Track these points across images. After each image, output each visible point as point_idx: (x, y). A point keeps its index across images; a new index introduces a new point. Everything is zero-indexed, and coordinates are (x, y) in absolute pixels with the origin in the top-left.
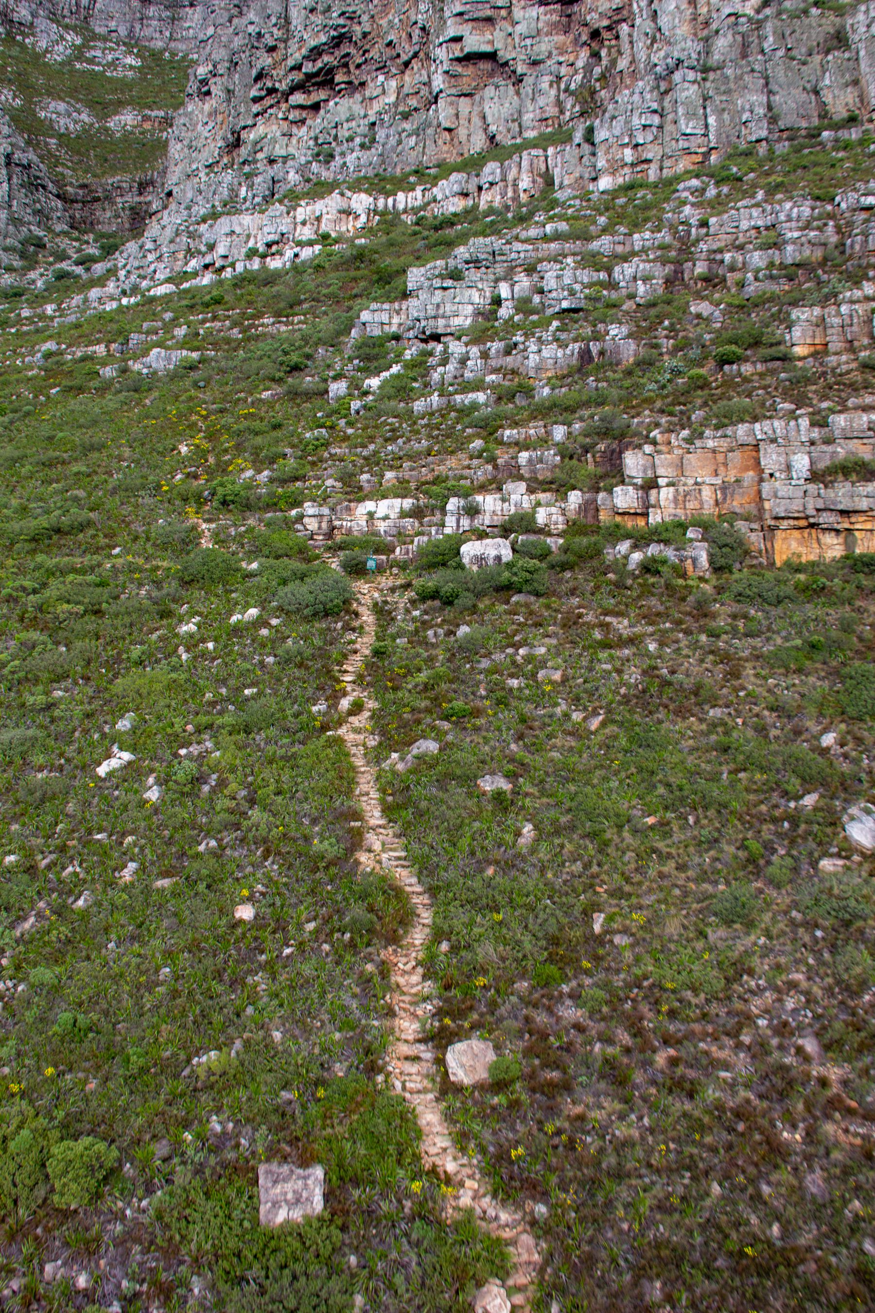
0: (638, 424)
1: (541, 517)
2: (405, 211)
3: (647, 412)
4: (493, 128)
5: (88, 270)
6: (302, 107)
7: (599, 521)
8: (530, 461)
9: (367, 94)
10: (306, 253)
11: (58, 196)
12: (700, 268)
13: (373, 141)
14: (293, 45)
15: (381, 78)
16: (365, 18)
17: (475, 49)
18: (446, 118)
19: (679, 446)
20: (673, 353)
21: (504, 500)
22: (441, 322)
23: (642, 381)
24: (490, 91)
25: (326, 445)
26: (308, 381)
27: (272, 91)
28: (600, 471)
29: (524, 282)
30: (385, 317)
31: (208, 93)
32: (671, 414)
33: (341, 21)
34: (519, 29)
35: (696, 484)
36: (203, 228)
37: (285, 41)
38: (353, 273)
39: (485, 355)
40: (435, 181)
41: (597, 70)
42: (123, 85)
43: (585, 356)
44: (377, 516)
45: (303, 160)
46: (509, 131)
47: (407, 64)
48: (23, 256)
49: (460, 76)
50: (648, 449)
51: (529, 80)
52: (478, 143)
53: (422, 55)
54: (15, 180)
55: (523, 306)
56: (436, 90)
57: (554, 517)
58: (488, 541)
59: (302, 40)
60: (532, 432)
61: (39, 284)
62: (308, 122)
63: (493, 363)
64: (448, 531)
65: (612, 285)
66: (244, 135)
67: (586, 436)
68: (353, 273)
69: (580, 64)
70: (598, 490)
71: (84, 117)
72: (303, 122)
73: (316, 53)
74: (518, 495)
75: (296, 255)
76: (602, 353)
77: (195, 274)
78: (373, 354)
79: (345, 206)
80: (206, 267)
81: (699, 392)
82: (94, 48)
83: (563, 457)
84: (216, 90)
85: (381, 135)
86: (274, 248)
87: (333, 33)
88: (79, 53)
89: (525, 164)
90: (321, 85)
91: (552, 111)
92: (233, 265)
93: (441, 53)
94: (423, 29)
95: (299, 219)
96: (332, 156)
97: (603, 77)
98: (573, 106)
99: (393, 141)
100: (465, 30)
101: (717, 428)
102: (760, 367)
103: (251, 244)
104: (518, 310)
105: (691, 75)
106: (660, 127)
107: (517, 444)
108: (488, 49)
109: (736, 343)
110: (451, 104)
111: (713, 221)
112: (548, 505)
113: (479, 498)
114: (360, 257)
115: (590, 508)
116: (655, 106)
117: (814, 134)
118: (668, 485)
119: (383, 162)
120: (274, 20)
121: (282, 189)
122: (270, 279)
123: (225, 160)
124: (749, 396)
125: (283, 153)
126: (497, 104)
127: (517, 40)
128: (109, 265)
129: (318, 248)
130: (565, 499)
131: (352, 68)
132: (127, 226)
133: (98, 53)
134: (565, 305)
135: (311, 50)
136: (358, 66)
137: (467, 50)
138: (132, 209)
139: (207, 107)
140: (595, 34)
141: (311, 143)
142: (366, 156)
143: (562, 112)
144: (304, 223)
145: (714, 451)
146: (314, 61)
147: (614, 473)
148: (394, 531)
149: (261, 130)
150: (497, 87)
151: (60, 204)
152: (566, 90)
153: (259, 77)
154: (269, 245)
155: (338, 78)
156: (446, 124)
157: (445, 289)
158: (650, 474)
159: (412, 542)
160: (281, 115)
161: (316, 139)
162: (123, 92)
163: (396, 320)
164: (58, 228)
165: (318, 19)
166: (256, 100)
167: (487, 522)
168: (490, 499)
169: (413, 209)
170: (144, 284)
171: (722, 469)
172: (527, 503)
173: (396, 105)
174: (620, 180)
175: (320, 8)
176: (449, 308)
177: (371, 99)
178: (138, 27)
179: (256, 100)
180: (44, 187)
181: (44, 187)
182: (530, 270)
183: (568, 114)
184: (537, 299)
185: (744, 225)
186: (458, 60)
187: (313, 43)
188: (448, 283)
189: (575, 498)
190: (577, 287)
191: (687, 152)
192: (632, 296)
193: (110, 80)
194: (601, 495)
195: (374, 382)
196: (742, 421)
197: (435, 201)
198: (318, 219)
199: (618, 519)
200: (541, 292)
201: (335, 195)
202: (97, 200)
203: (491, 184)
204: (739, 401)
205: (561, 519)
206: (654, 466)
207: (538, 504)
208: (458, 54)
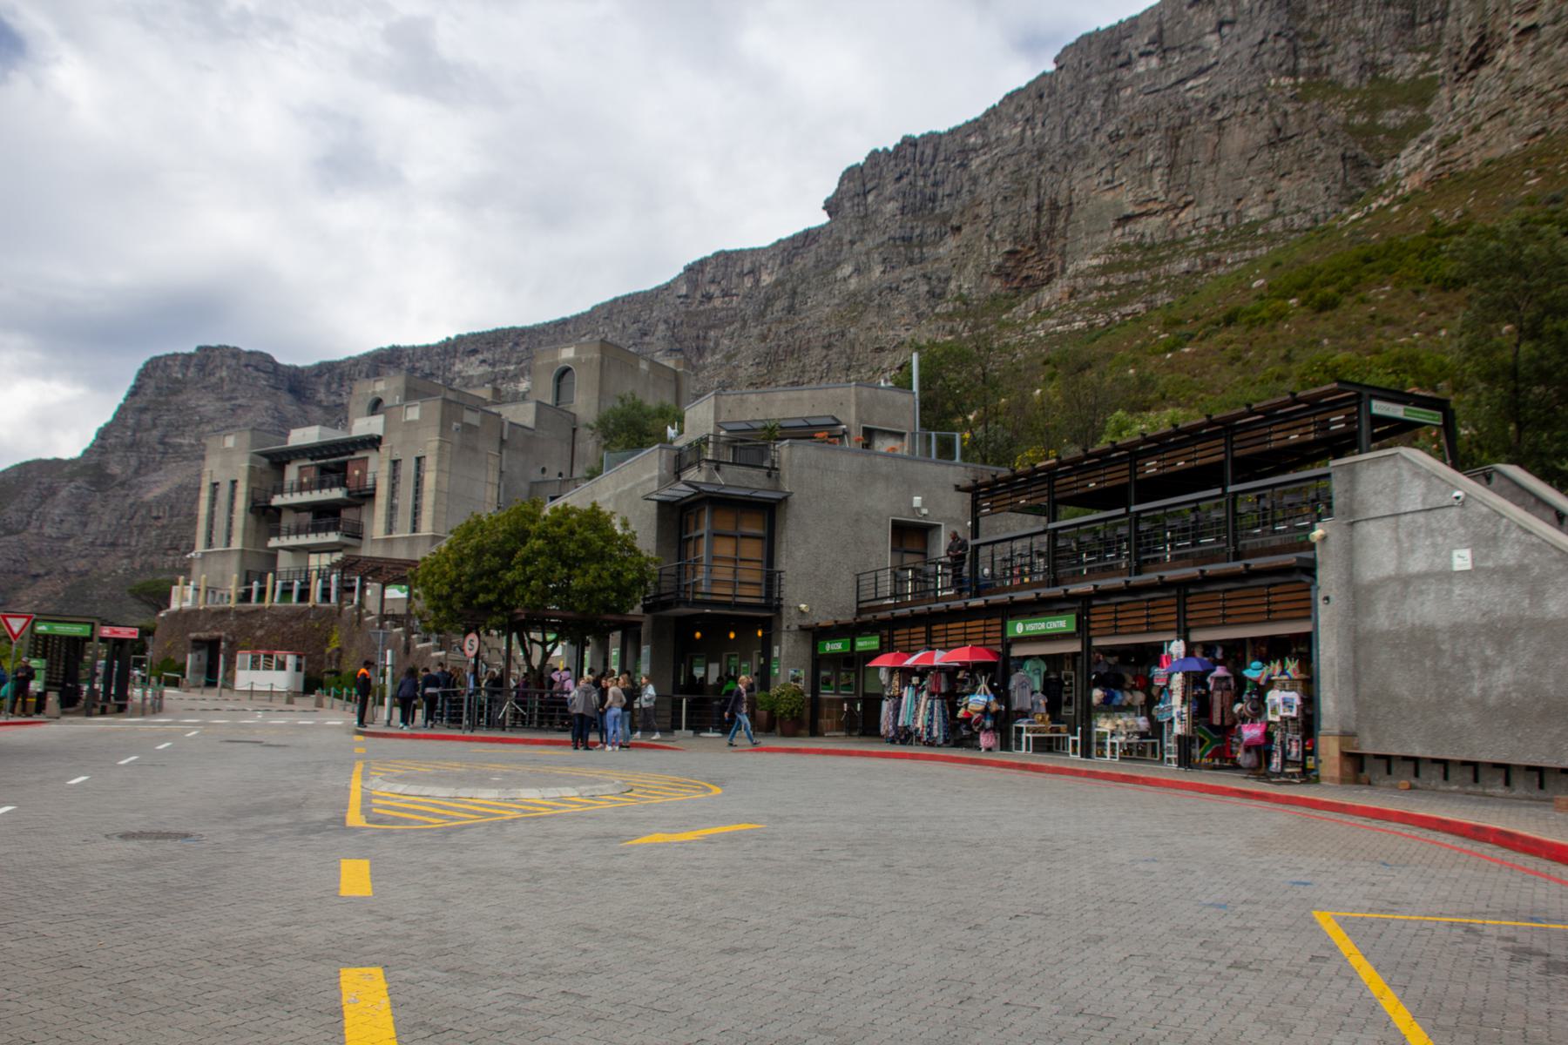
71: (1409, 113)
165: (1472, 32)
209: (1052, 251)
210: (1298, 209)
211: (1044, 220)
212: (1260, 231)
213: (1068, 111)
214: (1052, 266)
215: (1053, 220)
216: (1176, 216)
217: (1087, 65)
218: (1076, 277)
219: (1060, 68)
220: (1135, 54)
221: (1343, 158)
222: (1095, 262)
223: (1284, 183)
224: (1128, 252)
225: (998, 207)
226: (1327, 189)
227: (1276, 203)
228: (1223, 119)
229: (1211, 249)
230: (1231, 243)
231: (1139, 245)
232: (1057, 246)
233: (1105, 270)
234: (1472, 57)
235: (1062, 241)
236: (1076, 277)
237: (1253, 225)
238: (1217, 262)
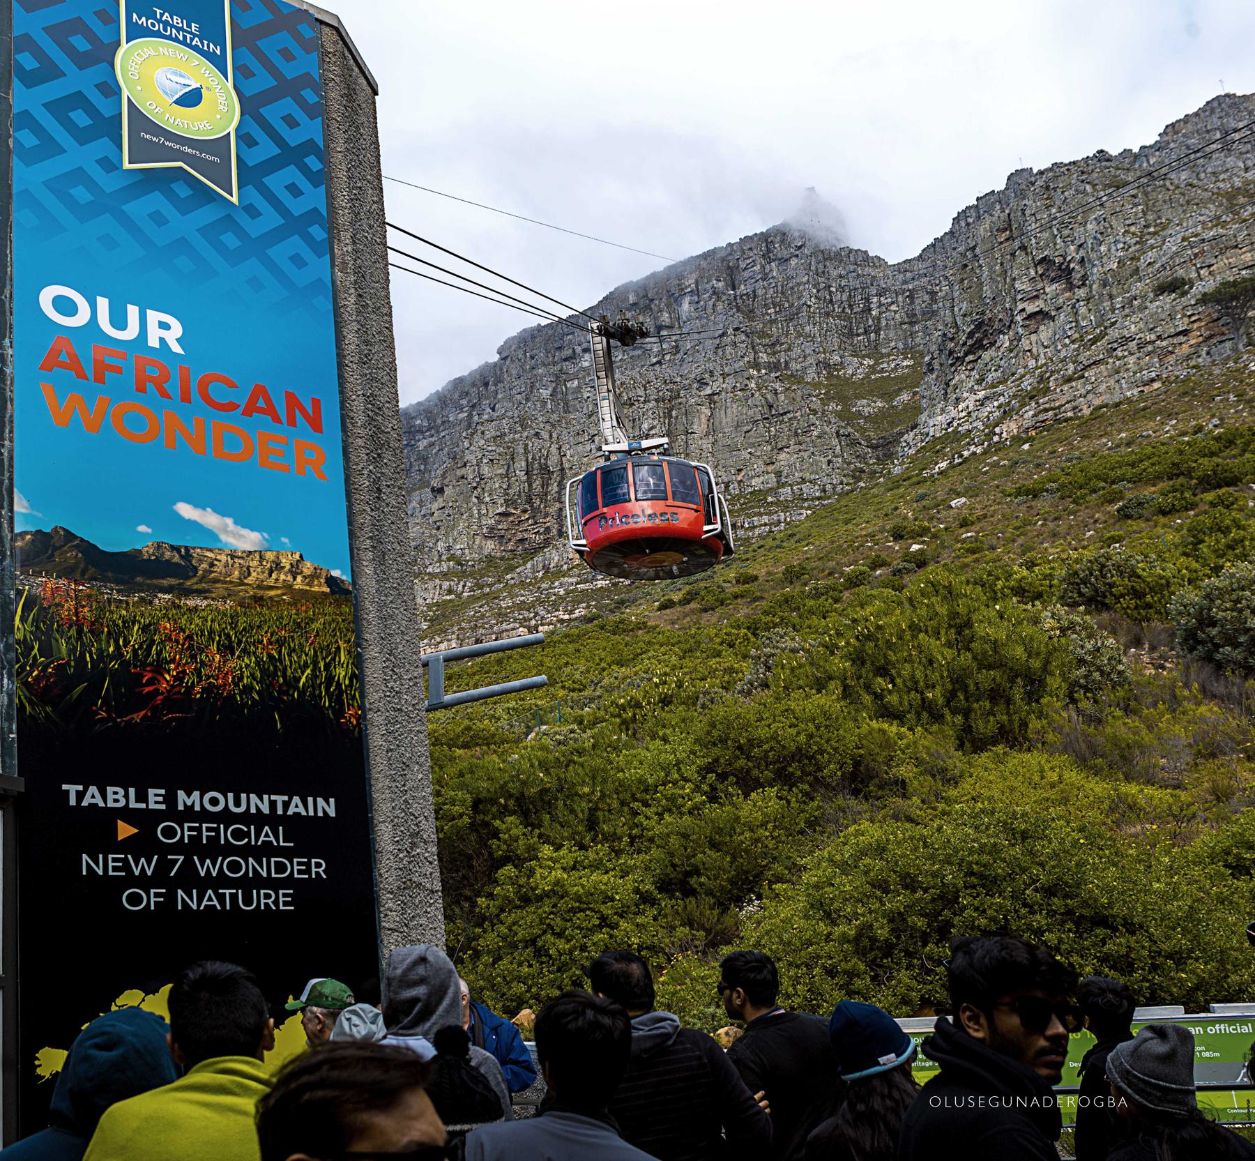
14: (961, 334)
24: (1042, 328)
27: (958, 358)
42: (902, 378)
48: (854, 477)
90: (979, 348)
93: (1019, 318)
133: (885, 365)
149: (957, 378)
165: (968, 319)
166: (952, 365)
179: (952, 365)
209: (547, 515)
211: (537, 484)
213: (519, 397)
214: (548, 530)
217: (532, 357)
220: (578, 349)
221: (837, 433)
223: (783, 456)
225: (486, 470)
226: (829, 462)
227: (778, 474)
228: (713, 394)
232: (553, 510)
234: (970, 342)
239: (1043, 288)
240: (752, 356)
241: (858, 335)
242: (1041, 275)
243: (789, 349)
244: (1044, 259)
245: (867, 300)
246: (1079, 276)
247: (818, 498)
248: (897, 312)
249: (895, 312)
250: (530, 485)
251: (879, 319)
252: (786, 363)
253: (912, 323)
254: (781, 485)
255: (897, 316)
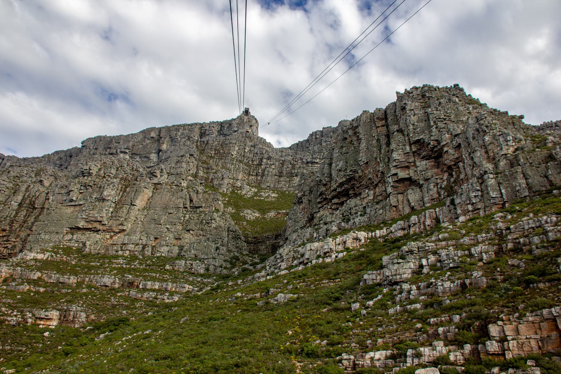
0: (493, 312)
1: (452, 358)
2: (380, 237)
3: (496, 307)
4: (413, 204)
5: (254, 267)
6: (337, 204)
7: (481, 358)
8: (444, 332)
9: (362, 196)
10: (341, 255)
11: (245, 242)
12: (510, 246)
13: (365, 213)
14: (333, 183)
15: (367, 191)
16: (360, 171)
17: (403, 177)
18: (394, 202)
19: (515, 321)
20: (504, 281)
21: (433, 350)
22: (398, 277)
23: (491, 294)
24: (410, 191)
25: (352, 329)
26: (343, 304)
27: (325, 199)
28: (477, 334)
29: (432, 258)
30: (374, 277)
31: (302, 202)
32: (508, 307)
33: (351, 173)
34: (419, 168)
35: (527, 338)
36: (300, 249)
37: (330, 182)
38: (359, 262)
39: (418, 288)
40: (391, 225)
41: (452, 180)
42: (271, 203)
43: (463, 286)
44: (375, 359)
45: (338, 222)
46: (419, 205)
47: (377, 185)
48: (231, 263)
49: (398, 187)
50: (500, 323)
51: (425, 186)
52: (407, 210)
53: (383, 181)
54: (230, 236)
55: (433, 267)
56: (389, 193)
57: (458, 357)
58: (428, 369)
59: (336, 180)
60: (443, 319)
61: (236, 273)
62: (340, 208)
63: (422, 292)
64: (408, 365)
65: (471, 255)
66: (315, 215)
67: (469, 319)
68: (359, 262)
69: (445, 178)
70: (478, 344)
71: (257, 215)
72: (337, 209)
73: (341, 184)
74: (440, 348)
75: (336, 257)
76: (470, 284)
77: (296, 266)
78: (370, 291)
79: (355, 237)
80: (300, 263)
81: (520, 297)
82: (261, 192)
83: (459, 329)
84: (305, 200)
85: (368, 210)
86: (327, 254)
87: (348, 177)
88: (256, 194)
89: (427, 215)
91: (436, 196)
92: (311, 262)
93: (390, 180)
94: (382, 172)
95: (337, 242)
96: (350, 220)
97: (455, 182)
98: (444, 193)
99: (373, 213)
100: (398, 171)
101: (532, 312)
102: (547, 284)
103: (318, 253)
104: (431, 270)
105: (491, 176)
106: (482, 196)
107: (437, 324)
108: (408, 176)
109: (534, 275)
110: (395, 197)
111: (512, 227)
112: (454, 351)
113: (422, 349)
114: (362, 256)
115: (475, 352)
116: (478, 188)
117: (549, 192)
118: (512, 340)
119: (370, 220)
120: (326, 175)
121: (330, 232)
122: (324, 266)
123: (308, 225)
124: (545, 297)
125: (330, 220)
126: (413, 196)
127: (419, 172)
128: (263, 265)
129: (345, 253)
130: (463, 348)
131: (356, 189)
132: (270, 251)
133: (263, 194)
134: (451, 265)
135: (340, 184)
136: (358, 188)
137: (400, 178)
138: (272, 245)
139: (301, 207)
140: (450, 168)
141: (341, 216)
142: (362, 219)
143: (440, 196)
144: (339, 244)
145: (533, 323)
146: (341, 187)
147: (485, 334)
148: (383, 366)
149: (322, 212)
150: (413, 189)
151: (246, 244)
152: (441, 188)
153: (321, 194)
154: (325, 253)
155: (350, 192)
156: (394, 204)
157: (399, 263)
158: (502, 335)
159: (392, 370)
160: (329, 207)
161: (343, 214)
162: (270, 205)
163: (379, 278)
164: (245, 253)
166: (319, 203)
167: (426, 360)
168: (427, 349)
169: (383, 236)
170: (276, 271)
171: (539, 331)
172: (444, 351)
173: (373, 199)
174: (468, 217)
175: (343, 170)
176: (401, 271)
177: (363, 198)
178: (277, 184)
179: (319, 203)
180: (240, 238)
181: (240, 238)
182: (435, 253)
183: (442, 196)
184: (439, 264)
185: (526, 227)
186: (396, 181)
187: (341, 181)
188: (400, 261)
189: (468, 348)
190: (456, 258)
191: (495, 204)
192: (481, 260)
193: (266, 202)
194: (480, 346)
195: (371, 303)
196: (544, 308)
197: (391, 232)
198: (345, 242)
199: (490, 357)
200: (440, 261)
201: (351, 233)
202: (260, 242)
203: (414, 224)
204: (539, 299)
205: (462, 358)
206: (504, 331)
207: (450, 351)
208: (396, 179)
210: (196, 258)
212: (168, 267)
214: (14, 247)
215: (27, 216)
216: (111, 237)
218: (18, 265)
219: (83, 146)
221: (228, 228)
222: (40, 256)
224: (68, 255)
226: (217, 248)
227: (181, 248)
229: (129, 271)
230: (145, 270)
231: (79, 251)
233: (44, 265)
234: (339, 190)
235: (29, 232)
236: (18, 265)
237: (163, 261)
238: (131, 284)
239: (414, 162)
240: (195, 172)
241: (252, 175)
242: (414, 152)
243: (216, 173)
244: (418, 141)
245: (261, 160)
246: (451, 157)
247: (202, 275)
248: (273, 170)
249: (273, 169)
250: (17, 213)
251: (264, 171)
252: (212, 179)
253: (280, 176)
254: (180, 257)
255: (274, 171)
